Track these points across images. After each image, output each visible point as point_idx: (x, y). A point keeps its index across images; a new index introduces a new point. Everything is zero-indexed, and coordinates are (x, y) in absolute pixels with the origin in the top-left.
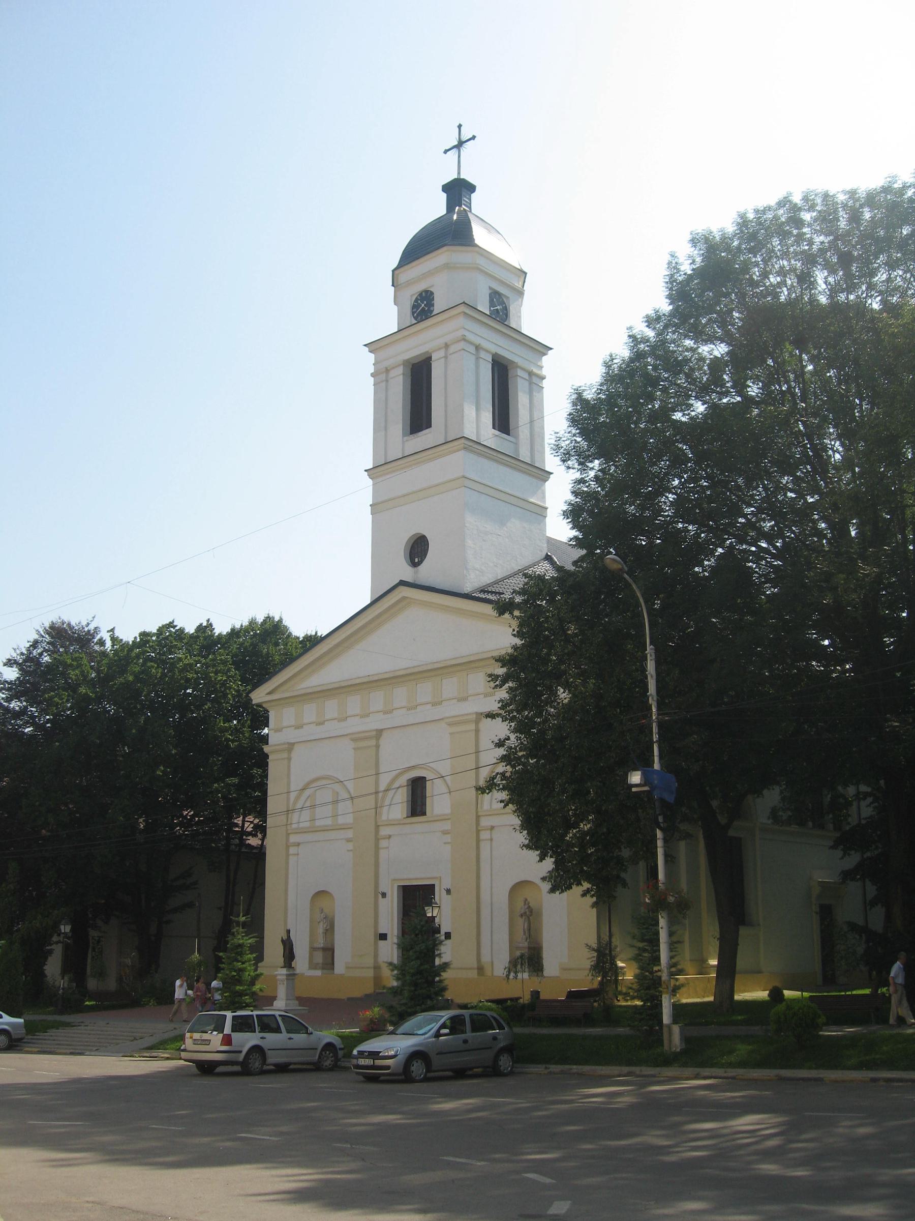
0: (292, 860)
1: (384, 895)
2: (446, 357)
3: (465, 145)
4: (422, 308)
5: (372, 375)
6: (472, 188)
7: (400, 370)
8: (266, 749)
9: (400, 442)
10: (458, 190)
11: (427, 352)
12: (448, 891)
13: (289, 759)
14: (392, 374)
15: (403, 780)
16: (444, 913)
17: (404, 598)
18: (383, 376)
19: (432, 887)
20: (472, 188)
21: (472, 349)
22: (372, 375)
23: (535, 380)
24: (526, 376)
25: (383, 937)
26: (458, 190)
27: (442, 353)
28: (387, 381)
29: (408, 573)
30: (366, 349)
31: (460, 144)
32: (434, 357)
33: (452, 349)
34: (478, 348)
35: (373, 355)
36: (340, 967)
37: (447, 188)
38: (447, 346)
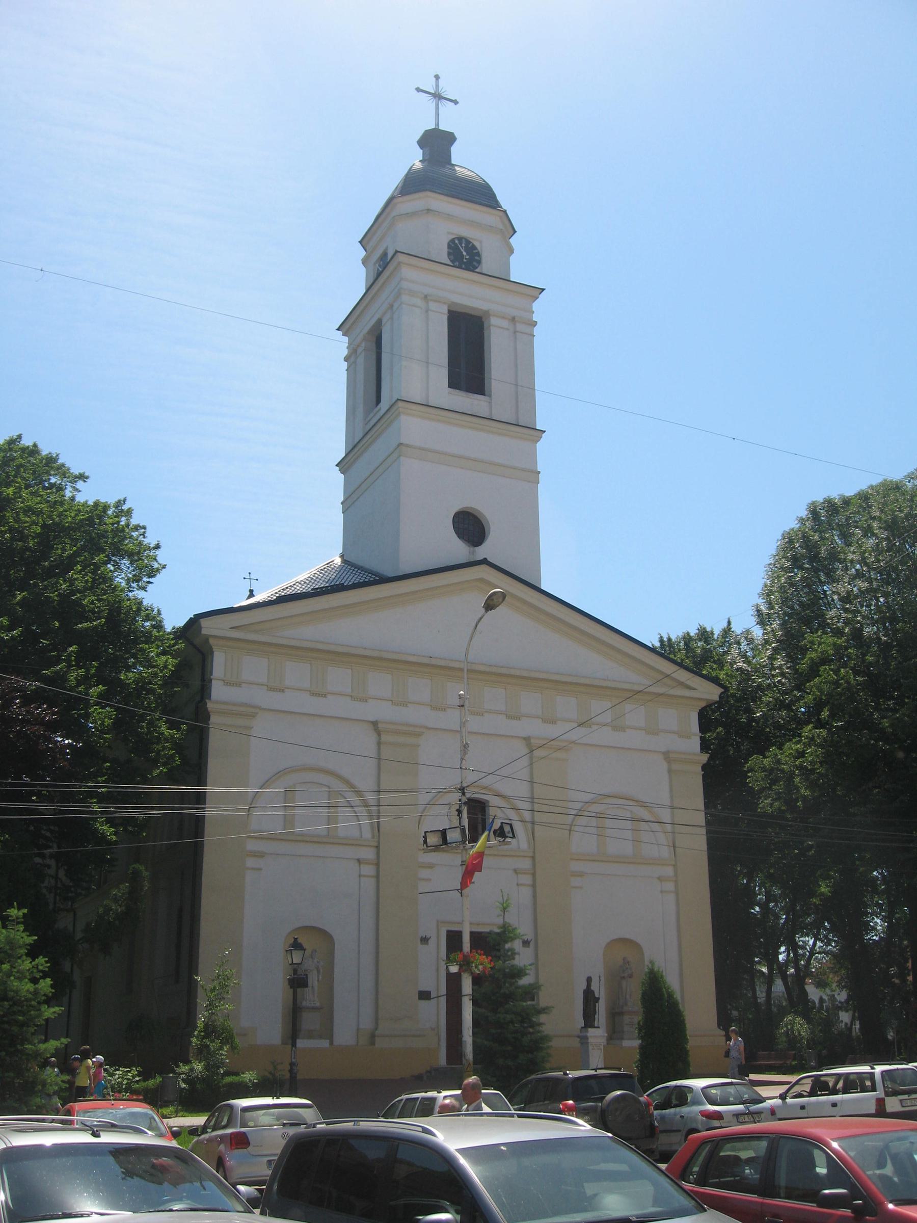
2: (392, 318)
5: (346, 359)
6: (450, 138)
10: (437, 143)
18: (352, 359)
20: (450, 138)
21: (419, 302)
22: (346, 359)
23: (520, 327)
24: (505, 323)
26: (437, 143)
27: (388, 315)
28: (355, 362)
30: (341, 333)
33: (395, 308)
34: (426, 297)
35: (346, 339)
37: (422, 143)
38: (391, 306)
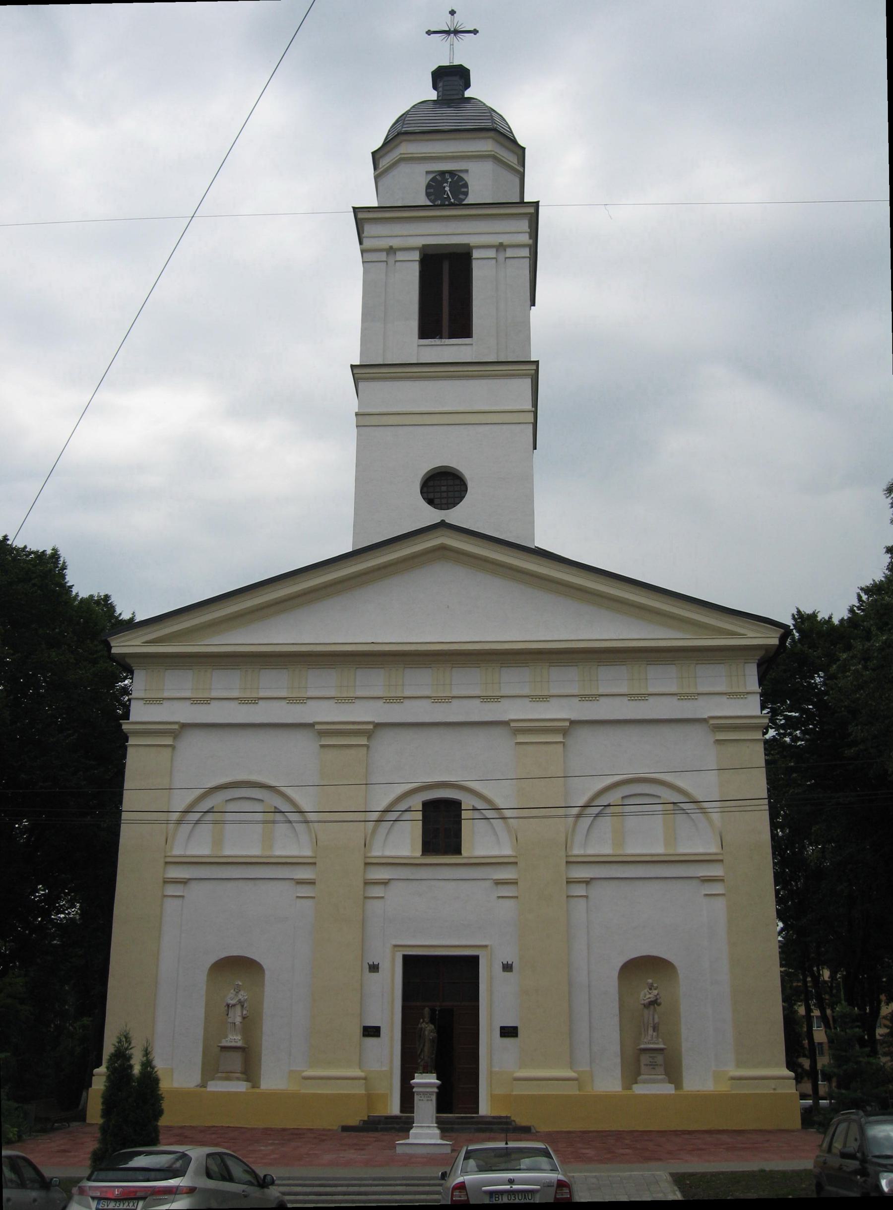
0: (171, 906)
1: (374, 968)
3: (461, 35)
4: (447, 192)
7: (416, 256)
8: (125, 727)
9: (407, 343)
11: (468, 244)
12: (507, 967)
13: (173, 747)
14: (400, 256)
15: (416, 802)
16: (497, 1000)
17: (443, 548)
19: (474, 961)
25: (372, 1032)
27: (492, 253)
29: (432, 515)
31: (456, 32)
32: (476, 254)
36: (274, 1079)
